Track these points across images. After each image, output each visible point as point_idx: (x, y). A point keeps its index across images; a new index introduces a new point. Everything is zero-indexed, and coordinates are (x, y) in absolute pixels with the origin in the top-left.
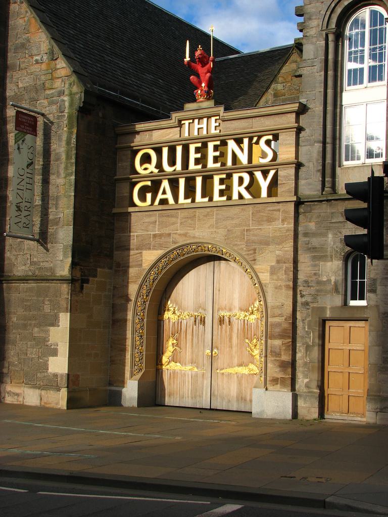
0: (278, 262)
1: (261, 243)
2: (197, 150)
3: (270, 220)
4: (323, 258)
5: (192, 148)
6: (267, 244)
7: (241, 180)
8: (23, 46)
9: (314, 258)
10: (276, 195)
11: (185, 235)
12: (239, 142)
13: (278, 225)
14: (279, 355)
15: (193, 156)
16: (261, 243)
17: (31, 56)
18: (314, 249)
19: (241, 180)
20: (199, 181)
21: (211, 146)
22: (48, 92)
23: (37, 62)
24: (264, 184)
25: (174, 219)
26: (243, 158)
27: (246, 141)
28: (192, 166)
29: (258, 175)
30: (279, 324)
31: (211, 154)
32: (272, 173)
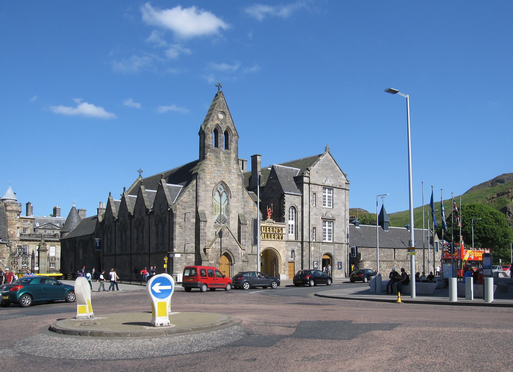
0: (283, 252)
1: (280, 248)
2: (268, 229)
3: (282, 244)
4: (288, 251)
5: (267, 228)
6: (281, 248)
7: (276, 236)
8: (247, 201)
9: (287, 251)
10: (282, 239)
11: (267, 245)
12: (276, 228)
13: (283, 245)
14: (283, 269)
15: (268, 229)
16: (280, 248)
17: (249, 204)
18: (287, 250)
19: (276, 236)
20: (269, 235)
21: (271, 228)
22: (254, 213)
23: (251, 206)
24: (280, 237)
25: (265, 242)
26: (277, 231)
27: (277, 228)
28: (268, 232)
29: (279, 235)
30: (284, 263)
31: (271, 230)
32: (281, 235)
